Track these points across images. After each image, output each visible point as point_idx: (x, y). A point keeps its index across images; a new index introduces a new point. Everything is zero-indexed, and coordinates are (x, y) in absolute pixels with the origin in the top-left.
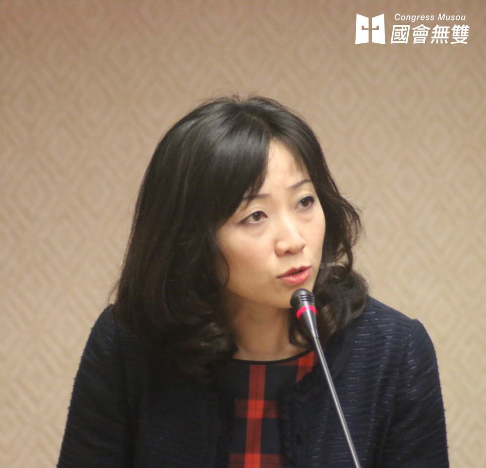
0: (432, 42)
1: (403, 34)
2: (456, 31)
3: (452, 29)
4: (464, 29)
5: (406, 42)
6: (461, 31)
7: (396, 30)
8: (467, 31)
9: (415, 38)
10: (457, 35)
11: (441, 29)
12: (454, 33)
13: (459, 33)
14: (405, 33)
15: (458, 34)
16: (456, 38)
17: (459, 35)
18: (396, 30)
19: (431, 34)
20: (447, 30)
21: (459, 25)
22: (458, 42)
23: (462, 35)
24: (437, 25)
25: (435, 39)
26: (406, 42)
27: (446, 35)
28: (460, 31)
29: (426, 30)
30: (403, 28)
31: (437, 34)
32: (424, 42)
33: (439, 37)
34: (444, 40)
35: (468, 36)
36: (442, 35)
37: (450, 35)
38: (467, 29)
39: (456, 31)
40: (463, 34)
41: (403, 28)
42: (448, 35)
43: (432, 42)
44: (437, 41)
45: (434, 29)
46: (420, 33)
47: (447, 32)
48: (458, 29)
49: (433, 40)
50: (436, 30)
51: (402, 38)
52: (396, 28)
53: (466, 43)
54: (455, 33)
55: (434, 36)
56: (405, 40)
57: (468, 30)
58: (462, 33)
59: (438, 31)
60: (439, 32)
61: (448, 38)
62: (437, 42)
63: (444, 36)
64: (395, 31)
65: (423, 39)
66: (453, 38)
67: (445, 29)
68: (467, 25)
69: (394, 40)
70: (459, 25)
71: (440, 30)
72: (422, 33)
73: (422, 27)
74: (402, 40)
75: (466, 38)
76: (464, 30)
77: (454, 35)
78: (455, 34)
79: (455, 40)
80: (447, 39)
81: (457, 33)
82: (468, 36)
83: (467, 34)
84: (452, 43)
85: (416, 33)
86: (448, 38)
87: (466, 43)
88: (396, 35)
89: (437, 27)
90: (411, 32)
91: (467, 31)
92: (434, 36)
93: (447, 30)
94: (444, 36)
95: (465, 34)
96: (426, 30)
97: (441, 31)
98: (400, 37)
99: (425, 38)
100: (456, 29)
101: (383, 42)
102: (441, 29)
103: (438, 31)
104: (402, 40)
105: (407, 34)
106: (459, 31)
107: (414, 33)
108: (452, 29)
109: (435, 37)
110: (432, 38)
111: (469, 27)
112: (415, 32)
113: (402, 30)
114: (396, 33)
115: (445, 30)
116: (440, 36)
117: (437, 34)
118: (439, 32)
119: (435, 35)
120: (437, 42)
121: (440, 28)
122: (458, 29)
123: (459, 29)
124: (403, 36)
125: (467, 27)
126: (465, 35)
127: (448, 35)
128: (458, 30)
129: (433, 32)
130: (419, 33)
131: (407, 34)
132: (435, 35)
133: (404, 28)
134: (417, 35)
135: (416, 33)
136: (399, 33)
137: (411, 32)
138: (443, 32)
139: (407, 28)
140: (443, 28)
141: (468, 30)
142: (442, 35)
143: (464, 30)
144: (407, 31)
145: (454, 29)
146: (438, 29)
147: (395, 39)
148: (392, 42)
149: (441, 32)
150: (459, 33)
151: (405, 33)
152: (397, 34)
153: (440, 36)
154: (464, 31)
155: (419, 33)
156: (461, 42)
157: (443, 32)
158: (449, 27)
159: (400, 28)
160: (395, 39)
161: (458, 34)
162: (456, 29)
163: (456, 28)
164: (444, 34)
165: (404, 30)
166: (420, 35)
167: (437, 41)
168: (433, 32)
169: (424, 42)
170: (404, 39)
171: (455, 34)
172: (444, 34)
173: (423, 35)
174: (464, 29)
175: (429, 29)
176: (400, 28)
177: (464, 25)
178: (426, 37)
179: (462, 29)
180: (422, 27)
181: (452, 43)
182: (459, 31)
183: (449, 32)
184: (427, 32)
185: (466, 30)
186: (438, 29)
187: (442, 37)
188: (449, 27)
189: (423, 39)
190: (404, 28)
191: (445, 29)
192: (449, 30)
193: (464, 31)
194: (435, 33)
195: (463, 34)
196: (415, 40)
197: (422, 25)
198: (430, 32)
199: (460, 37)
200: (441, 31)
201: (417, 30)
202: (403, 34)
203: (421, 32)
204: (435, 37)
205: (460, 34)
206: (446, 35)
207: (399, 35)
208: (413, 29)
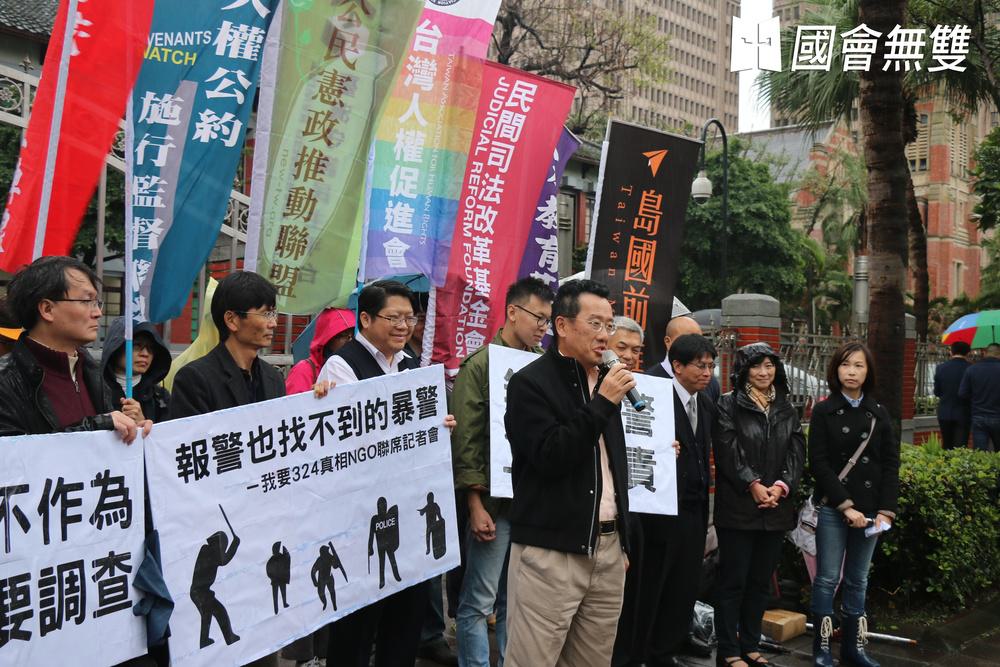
0: (885, 68)
1: (821, 46)
2: (940, 41)
3: (932, 36)
4: (959, 34)
5: (827, 68)
6: (951, 39)
7: (804, 37)
8: (965, 41)
9: (848, 57)
10: (942, 51)
11: (907, 35)
12: (936, 44)
13: (947, 45)
14: (825, 45)
15: (945, 48)
16: (940, 59)
17: (947, 51)
18: (804, 37)
19: (883, 49)
20: (919, 37)
21: (947, 27)
22: (946, 66)
23: (953, 51)
24: (898, 26)
25: (893, 61)
26: (827, 68)
27: (917, 50)
28: (950, 42)
29: (872, 37)
30: (819, 33)
31: (897, 48)
32: (867, 69)
33: (901, 56)
34: (912, 61)
35: (967, 51)
36: (909, 50)
37: (926, 51)
38: (966, 34)
39: (940, 41)
40: (957, 48)
41: (819, 33)
42: (922, 50)
43: (885, 68)
44: (897, 63)
45: (889, 36)
46: (859, 46)
47: (919, 43)
48: (944, 34)
49: (889, 62)
50: (895, 39)
51: (818, 56)
52: (804, 33)
53: (962, 69)
54: (939, 45)
55: (890, 53)
56: (825, 64)
57: (968, 38)
58: (954, 44)
59: (899, 39)
60: (902, 44)
61: (921, 56)
62: (897, 68)
63: (913, 51)
64: (801, 41)
65: (865, 59)
66: (934, 57)
67: (915, 35)
68: (965, 27)
69: (798, 63)
70: (947, 27)
71: (903, 37)
72: (863, 45)
73: (863, 31)
74: (818, 62)
75: (964, 57)
76: (959, 38)
77: (935, 51)
78: (938, 48)
79: (937, 64)
80: (920, 60)
81: (944, 45)
82: (967, 51)
83: (964, 48)
84: (931, 70)
85: (849, 46)
86: (921, 56)
87: (962, 69)
88: (803, 51)
89: (897, 30)
90: (839, 41)
91: (964, 48)
92: (890, 53)
93: (919, 37)
94: (913, 51)
95: (961, 48)
96: (872, 37)
97: (907, 39)
98: (814, 54)
99: (869, 57)
100: (940, 34)
101: (778, 68)
102: (907, 35)
103: (899, 39)
104: (818, 62)
105: (828, 46)
106: (946, 41)
107: (845, 46)
108: (932, 36)
109: (892, 55)
110: (886, 56)
111: (969, 31)
112: (846, 42)
113: (818, 37)
114: (804, 44)
115: (915, 39)
116: (905, 52)
117: (897, 48)
118: (902, 44)
119: (893, 50)
120: (897, 68)
121: (904, 32)
122: (944, 34)
123: (948, 34)
124: (819, 53)
125: (966, 30)
126: (961, 51)
127: (922, 50)
128: (944, 38)
129: (887, 44)
130: (856, 45)
131: (828, 46)
132: (893, 50)
133: (822, 34)
134: (853, 49)
135: (849, 46)
136: (811, 44)
137: (839, 41)
138: (910, 44)
139: (829, 31)
140: (911, 32)
141: (967, 44)
142: (909, 50)
143: (959, 38)
144: (828, 41)
145: (935, 35)
146: (899, 36)
147: (801, 59)
148: (795, 67)
149: (906, 44)
150: (947, 45)
151: (825, 45)
152: (807, 48)
153: (905, 52)
154: (958, 41)
155: (856, 45)
156: (952, 67)
157: (910, 44)
158: (924, 31)
159: (814, 32)
160: (801, 59)
161: (945, 48)
162: (940, 34)
163: (940, 33)
164: (913, 48)
165: (823, 38)
166: (859, 49)
167: (897, 63)
168: (887, 44)
169: (867, 69)
170: (822, 61)
171: (938, 48)
172: (913, 48)
173: (866, 49)
174: (959, 34)
175: (878, 34)
176: (814, 32)
177: (958, 26)
178: (873, 55)
179: (954, 35)
180: (863, 31)
181: (931, 70)
182: (946, 41)
183: (923, 44)
184: (875, 42)
185: (963, 38)
186: (899, 36)
187: (909, 55)
188: (924, 31)
189: (865, 59)
190: (822, 34)
191: (915, 35)
192: (923, 40)
193: (958, 41)
194: (893, 44)
195: (957, 48)
196: (847, 62)
197: (863, 26)
198: (882, 41)
199: (949, 54)
200: (907, 39)
201: (848, 37)
202: (821, 46)
203: (860, 42)
204: (892, 55)
205: (949, 48)
206: (917, 50)
207: (811, 51)
208: (843, 35)
